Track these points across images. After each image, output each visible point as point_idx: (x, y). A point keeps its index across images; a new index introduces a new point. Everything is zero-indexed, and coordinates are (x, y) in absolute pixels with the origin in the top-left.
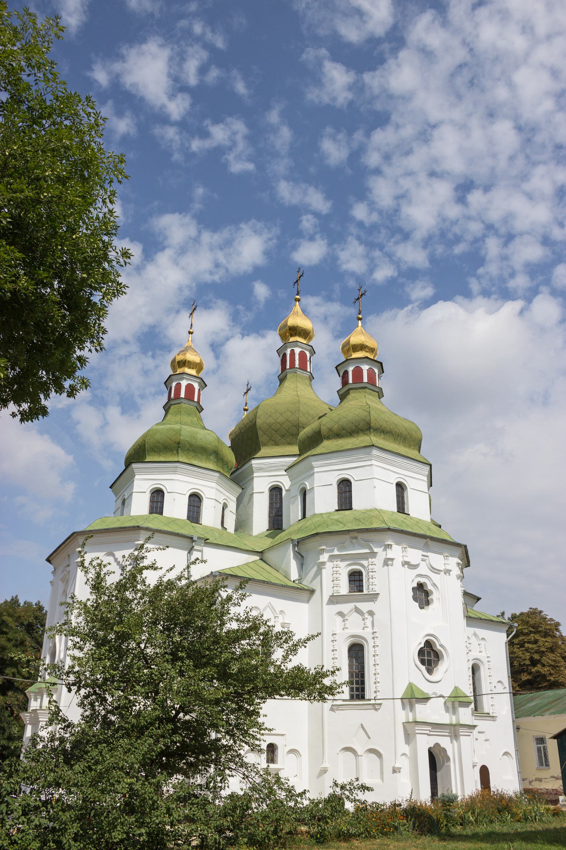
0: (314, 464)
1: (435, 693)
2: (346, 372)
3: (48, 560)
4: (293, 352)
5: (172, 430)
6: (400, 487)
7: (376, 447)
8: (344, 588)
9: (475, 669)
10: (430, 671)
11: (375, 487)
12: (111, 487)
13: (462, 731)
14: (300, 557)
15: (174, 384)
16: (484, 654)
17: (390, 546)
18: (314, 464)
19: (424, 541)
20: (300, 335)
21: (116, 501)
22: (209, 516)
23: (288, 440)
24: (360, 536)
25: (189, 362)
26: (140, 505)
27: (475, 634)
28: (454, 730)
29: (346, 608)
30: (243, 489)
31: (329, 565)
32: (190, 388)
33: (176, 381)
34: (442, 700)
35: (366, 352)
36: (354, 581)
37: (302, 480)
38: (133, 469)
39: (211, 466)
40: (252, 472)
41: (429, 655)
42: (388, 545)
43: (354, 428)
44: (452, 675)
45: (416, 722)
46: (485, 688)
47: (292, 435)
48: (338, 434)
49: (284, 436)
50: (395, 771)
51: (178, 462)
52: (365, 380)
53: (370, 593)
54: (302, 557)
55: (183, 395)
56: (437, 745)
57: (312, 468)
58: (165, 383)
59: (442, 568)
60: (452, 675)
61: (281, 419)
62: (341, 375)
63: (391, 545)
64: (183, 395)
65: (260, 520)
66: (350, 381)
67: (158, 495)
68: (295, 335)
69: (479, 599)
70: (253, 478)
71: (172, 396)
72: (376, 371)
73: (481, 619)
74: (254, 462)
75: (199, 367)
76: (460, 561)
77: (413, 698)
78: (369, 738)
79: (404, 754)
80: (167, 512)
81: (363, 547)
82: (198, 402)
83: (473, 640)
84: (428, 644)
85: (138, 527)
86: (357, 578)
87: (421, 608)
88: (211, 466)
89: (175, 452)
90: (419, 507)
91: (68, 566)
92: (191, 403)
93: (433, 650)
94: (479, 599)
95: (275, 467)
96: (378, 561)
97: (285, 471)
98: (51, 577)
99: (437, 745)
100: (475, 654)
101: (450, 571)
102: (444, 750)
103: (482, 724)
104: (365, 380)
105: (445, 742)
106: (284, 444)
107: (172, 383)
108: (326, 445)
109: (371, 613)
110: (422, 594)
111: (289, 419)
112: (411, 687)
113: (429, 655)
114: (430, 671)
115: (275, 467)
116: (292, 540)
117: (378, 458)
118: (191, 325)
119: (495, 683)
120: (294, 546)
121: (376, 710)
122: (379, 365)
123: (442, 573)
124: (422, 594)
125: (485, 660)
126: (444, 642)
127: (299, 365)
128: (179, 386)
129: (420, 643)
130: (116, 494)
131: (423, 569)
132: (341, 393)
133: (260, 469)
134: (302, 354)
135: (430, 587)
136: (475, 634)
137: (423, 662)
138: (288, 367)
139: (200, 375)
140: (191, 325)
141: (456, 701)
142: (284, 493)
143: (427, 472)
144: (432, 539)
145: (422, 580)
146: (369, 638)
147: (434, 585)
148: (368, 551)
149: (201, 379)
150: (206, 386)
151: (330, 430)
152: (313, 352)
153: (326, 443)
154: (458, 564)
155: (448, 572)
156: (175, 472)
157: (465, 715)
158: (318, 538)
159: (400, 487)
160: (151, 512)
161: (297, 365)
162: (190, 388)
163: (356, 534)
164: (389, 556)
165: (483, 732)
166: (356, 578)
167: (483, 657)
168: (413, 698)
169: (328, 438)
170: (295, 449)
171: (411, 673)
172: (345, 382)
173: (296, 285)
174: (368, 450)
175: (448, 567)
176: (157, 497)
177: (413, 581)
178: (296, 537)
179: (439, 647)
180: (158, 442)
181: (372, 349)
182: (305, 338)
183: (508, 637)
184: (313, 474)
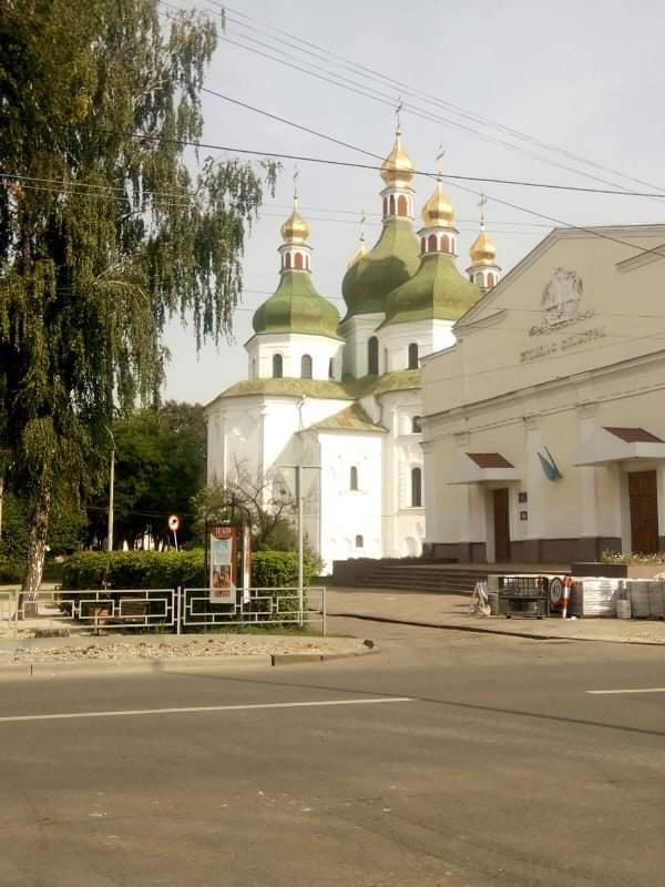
4: (392, 197)
5: (284, 303)
22: (320, 372)
26: (266, 370)
40: (354, 326)
55: (293, 265)
65: (362, 370)
67: (278, 360)
70: (354, 332)
75: (304, 234)
82: (307, 269)
160: (274, 376)
174: (429, 321)
176: (278, 360)
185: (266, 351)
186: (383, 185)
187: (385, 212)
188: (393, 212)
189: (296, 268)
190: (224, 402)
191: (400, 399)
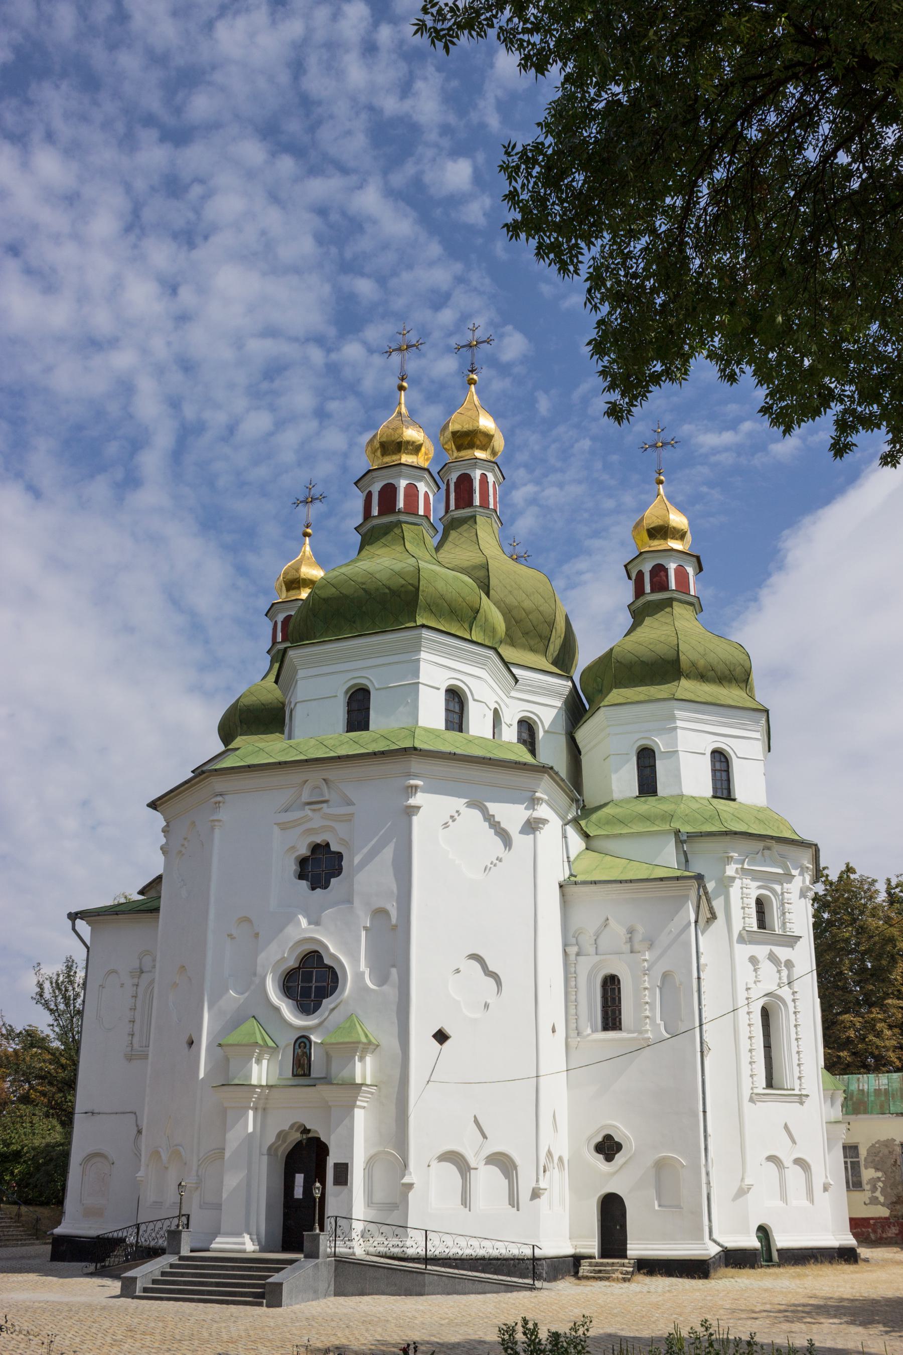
0: (678, 713)
4: (484, 477)
14: (683, 860)
18: (678, 713)
23: (532, 643)
24: (777, 847)
33: (407, 477)
38: (421, 638)
43: (727, 672)
47: (540, 637)
48: (703, 675)
49: (527, 633)
53: (788, 933)
57: (673, 718)
61: (527, 604)
78: (794, 1142)
81: (774, 864)
89: (466, 626)
95: (529, 686)
106: (523, 647)
108: (686, 687)
111: (541, 609)
115: (529, 686)
116: (677, 833)
121: (802, 1103)
142: (541, 734)
148: (780, 871)
151: (694, 664)
153: (684, 682)
156: (482, 665)
158: (728, 838)
163: (773, 843)
169: (688, 677)
178: (686, 829)
180: (442, 597)
184: (675, 728)
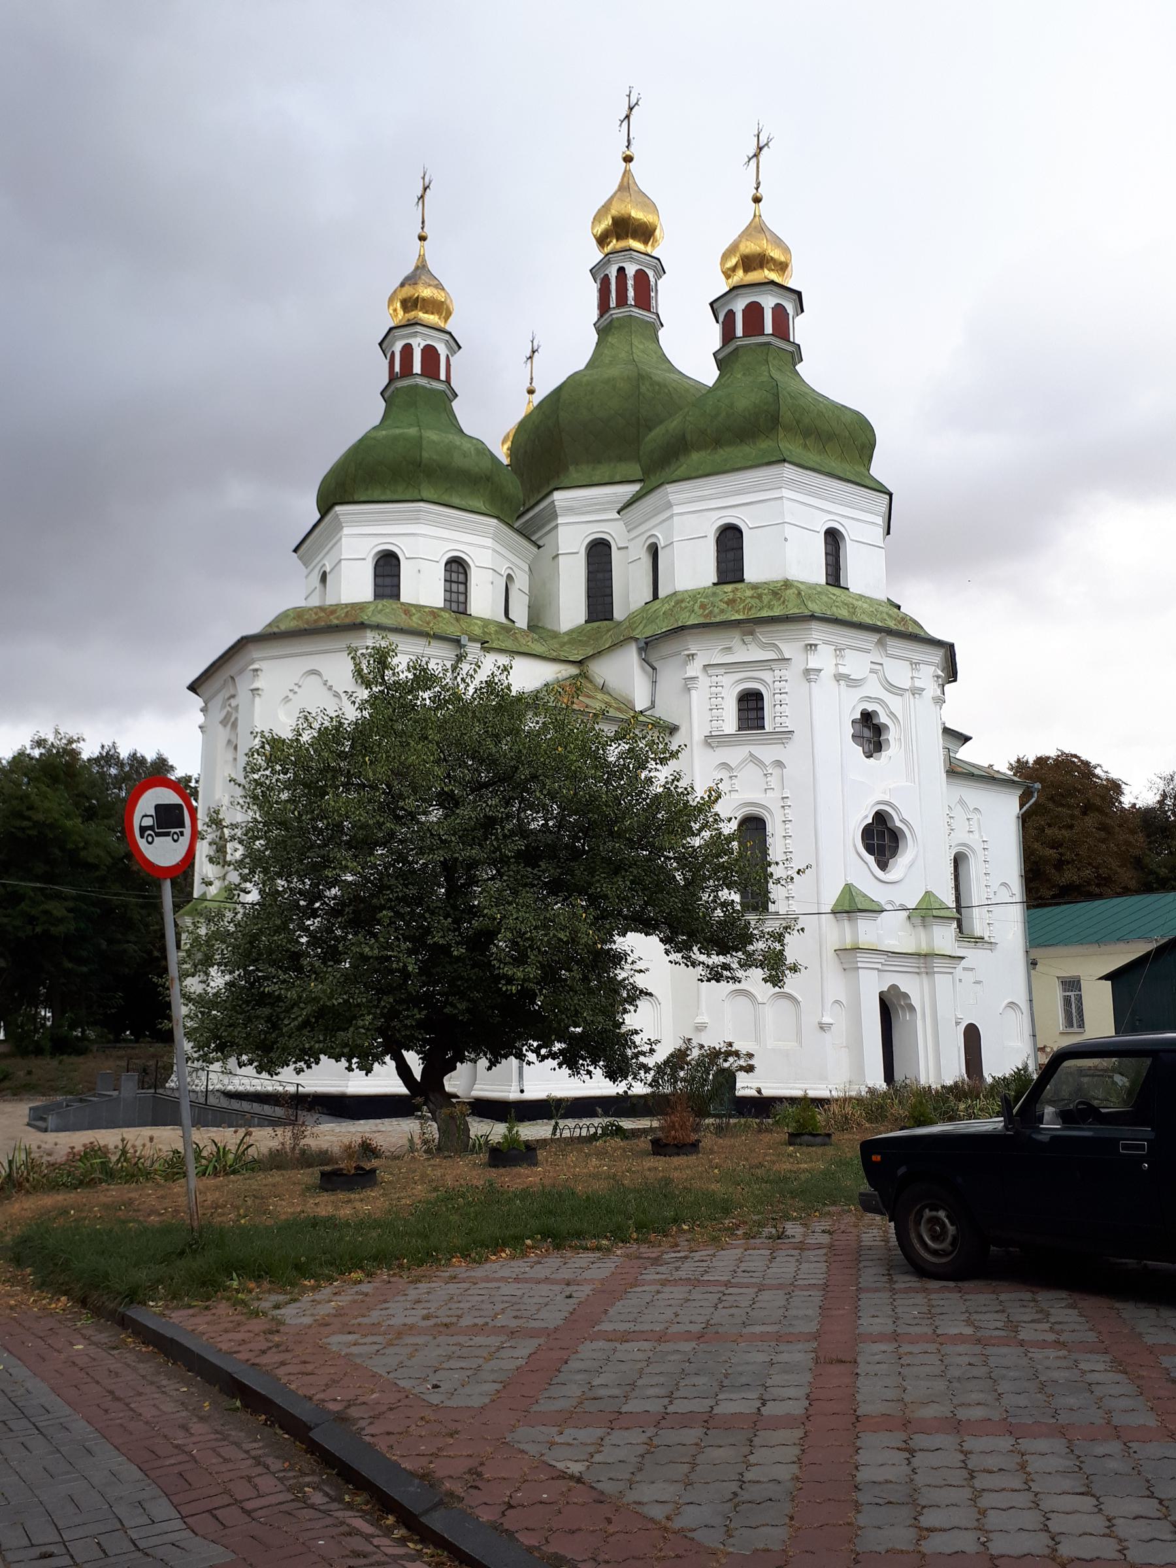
1: (890, 902)
2: (731, 314)
3: (193, 688)
6: (833, 538)
7: (790, 463)
8: (729, 722)
9: (959, 861)
10: (883, 866)
11: (786, 540)
12: (295, 551)
13: (937, 962)
15: (398, 347)
16: (976, 836)
17: (812, 647)
19: (875, 637)
20: (634, 238)
21: (307, 577)
22: (483, 601)
25: (424, 300)
26: (355, 585)
27: (961, 802)
28: (925, 960)
29: (734, 755)
30: (539, 547)
31: (704, 681)
32: (430, 354)
34: (905, 914)
35: (770, 270)
36: (748, 710)
37: (649, 530)
39: (483, 509)
40: (554, 515)
41: (882, 838)
42: (811, 645)
44: (919, 871)
45: (856, 949)
46: (976, 894)
50: (823, 1027)
51: (422, 500)
52: (769, 329)
54: (654, 669)
55: (417, 368)
56: (894, 987)
58: (380, 344)
59: (907, 685)
60: (919, 871)
62: (721, 319)
63: (816, 645)
64: (417, 368)
66: (739, 332)
67: (387, 566)
68: (626, 237)
69: (967, 739)
71: (397, 369)
72: (790, 308)
73: (973, 775)
74: (557, 496)
76: (940, 673)
77: (851, 906)
79: (837, 1002)
80: (406, 596)
82: (448, 381)
83: (958, 812)
84: (881, 818)
85: (362, 623)
86: (752, 704)
87: (869, 756)
88: (479, 504)
90: (865, 575)
91: (233, 696)
92: (436, 385)
93: (889, 829)
94: (967, 739)
96: (792, 673)
97: (619, 513)
98: (200, 718)
99: (894, 987)
100: (961, 836)
101: (923, 690)
102: (906, 996)
103: (973, 955)
104: (769, 329)
105: (909, 985)
107: (393, 344)
109: (779, 764)
110: (870, 732)
112: (849, 889)
113: (882, 838)
114: (883, 866)
116: (636, 640)
117: (793, 484)
118: (423, 222)
119: (995, 886)
120: (640, 650)
122: (795, 297)
123: (908, 694)
124: (870, 732)
125: (978, 847)
126: (905, 815)
127: (635, 299)
128: (407, 350)
129: (866, 817)
130: (306, 564)
131: (873, 688)
132: (719, 357)
133: (570, 510)
134: (641, 276)
135: (883, 719)
136: (961, 802)
137: (870, 849)
138: (613, 304)
139: (448, 328)
140: (423, 222)
141: (925, 913)
143: (884, 509)
144: (890, 632)
145: (870, 707)
146: (775, 807)
147: (892, 715)
148: (771, 655)
149: (450, 334)
150: (460, 347)
152: (661, 271)
153: (695, 456)
154: (938, 677)
155: (916, 691)
156: (416, 520)
157: (944, 938)
159: (833, 538)
160: (377, 596)
161: (631, 301)
162: (430, 354)
164: (811, 665)
165: (972, 969)
166: (751, 707)
167: (974, 840)
168: (851, 906)
170: (635, 470)
171: (850, 865)
172: (728, 334)
173: (625, 123)
175: (918, 683)
176: (387, 566)
177: (854, 708)
179: (898, 824)
181: (781, 263)
182: (646, 243)
183: (1021, 807)
184: (672, 516)
185: (361, 535)
186: (597, 255)
187: (604, 307)
188: (622, 301)
189: (424, 374)
190: (255, 652)
191: (707, 650)
